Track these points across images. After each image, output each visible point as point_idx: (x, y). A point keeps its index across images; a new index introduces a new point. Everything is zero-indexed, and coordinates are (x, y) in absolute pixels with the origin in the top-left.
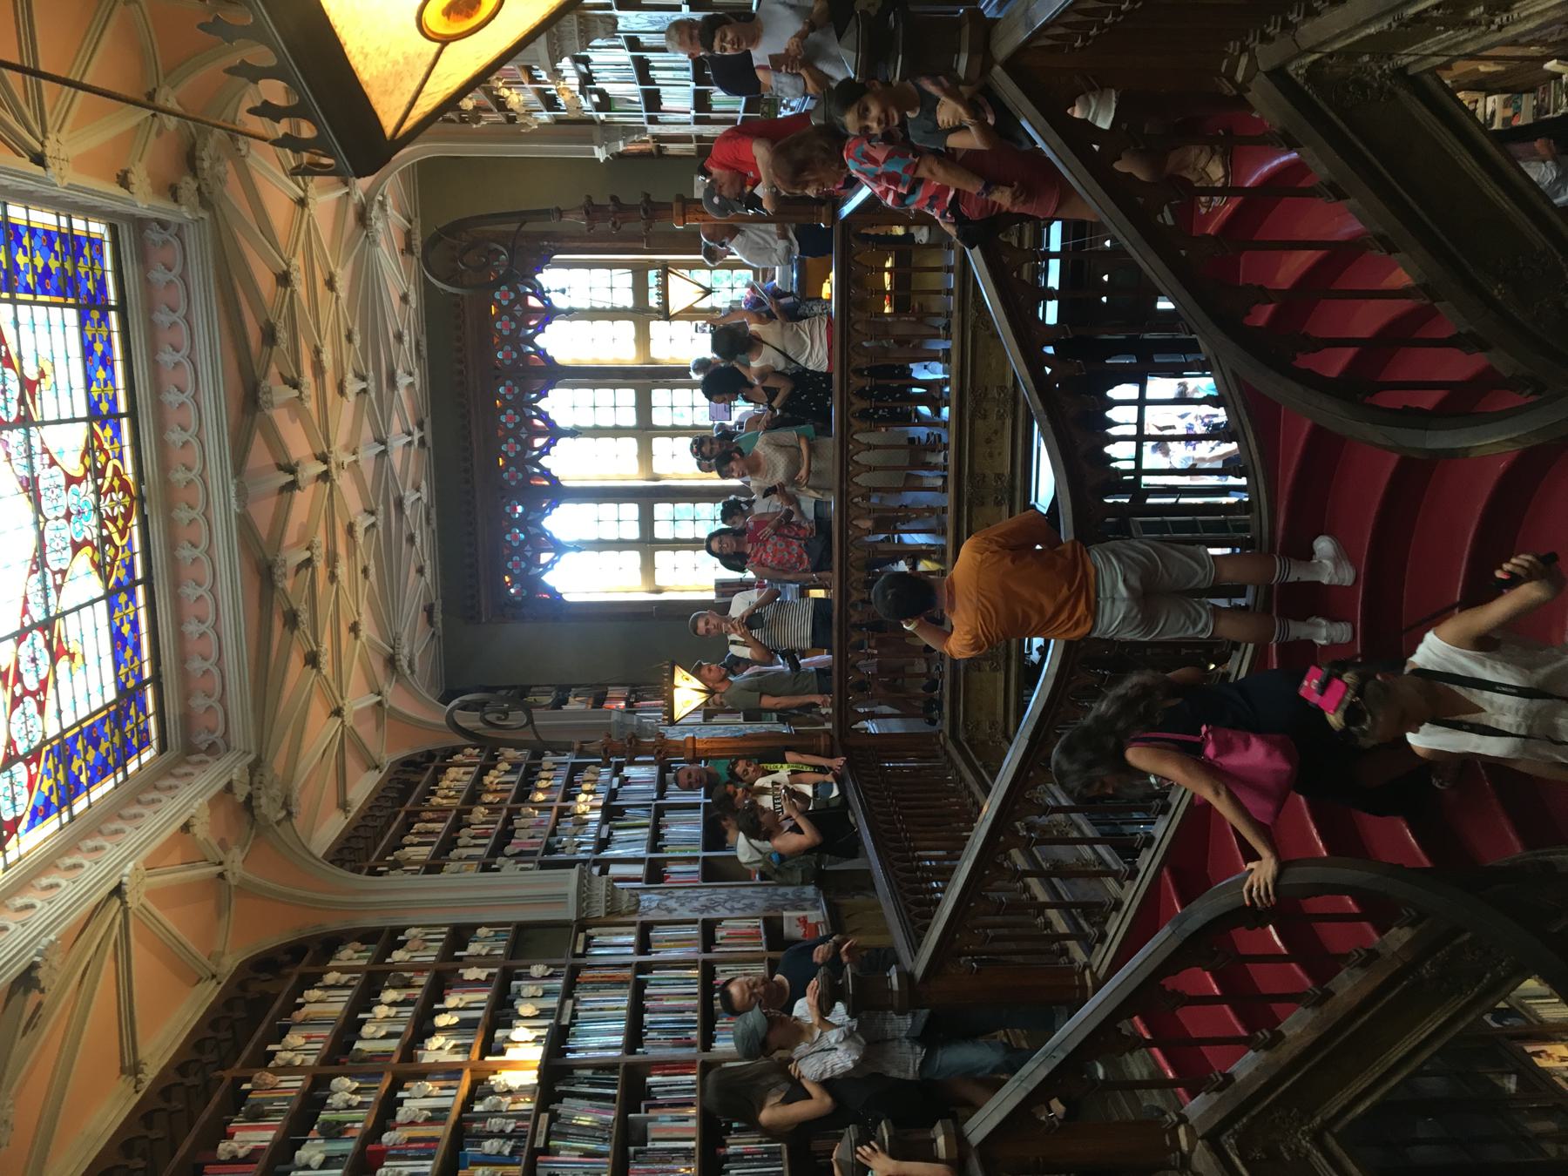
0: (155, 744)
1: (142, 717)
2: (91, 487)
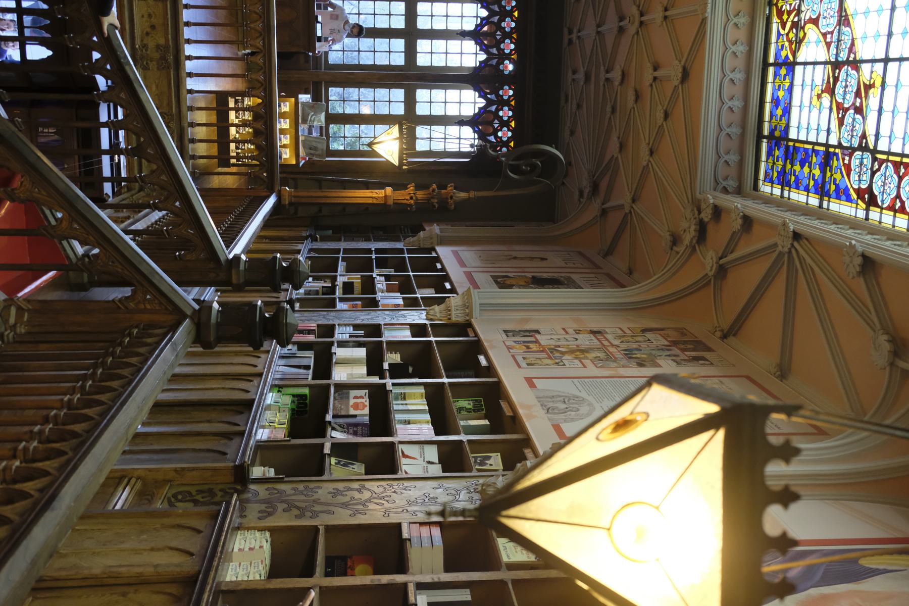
2: (802, 16)
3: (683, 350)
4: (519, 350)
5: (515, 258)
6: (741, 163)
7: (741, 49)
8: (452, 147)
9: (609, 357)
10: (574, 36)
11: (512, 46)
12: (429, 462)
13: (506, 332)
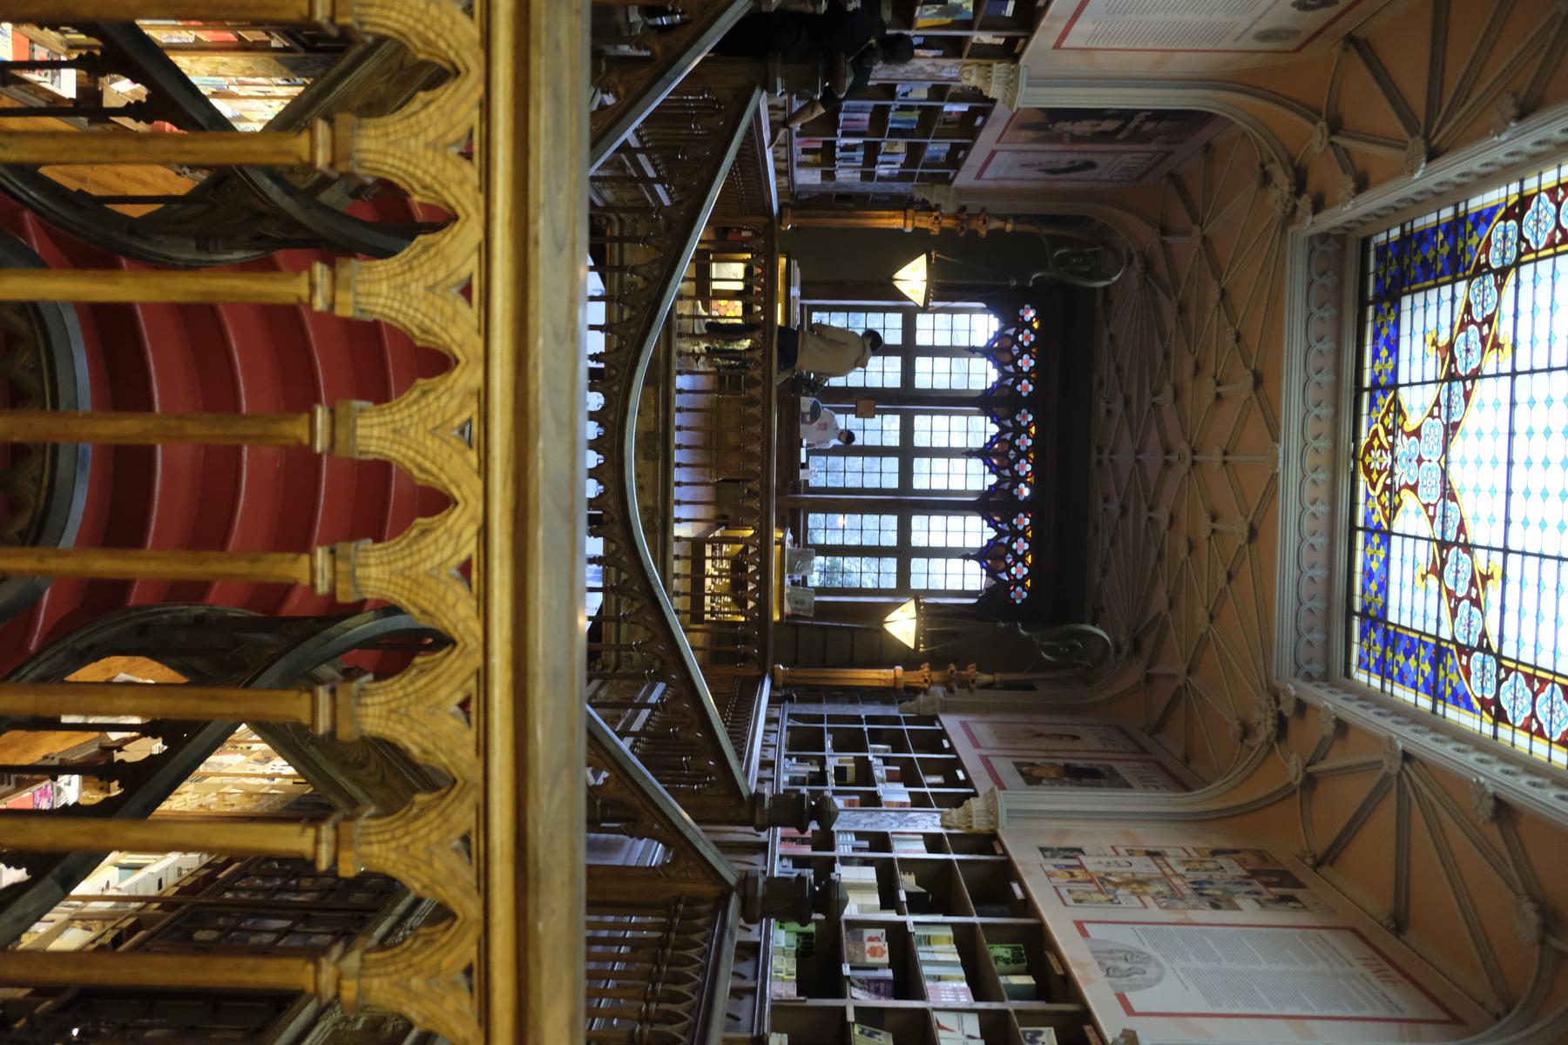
0: (1372, 247)
1: (1381, 273)
2: (1396, 479)
3: (1267, 885)
4: (1061, 878)
5: (1040, 735)
6: (1328, 643)
7: (1322, 509)
8: (954, 584)
9: (1175, 895)
10: (1106, 457)
11: (1029, 468)
12: (970, 1037)
13: (1042, 850)
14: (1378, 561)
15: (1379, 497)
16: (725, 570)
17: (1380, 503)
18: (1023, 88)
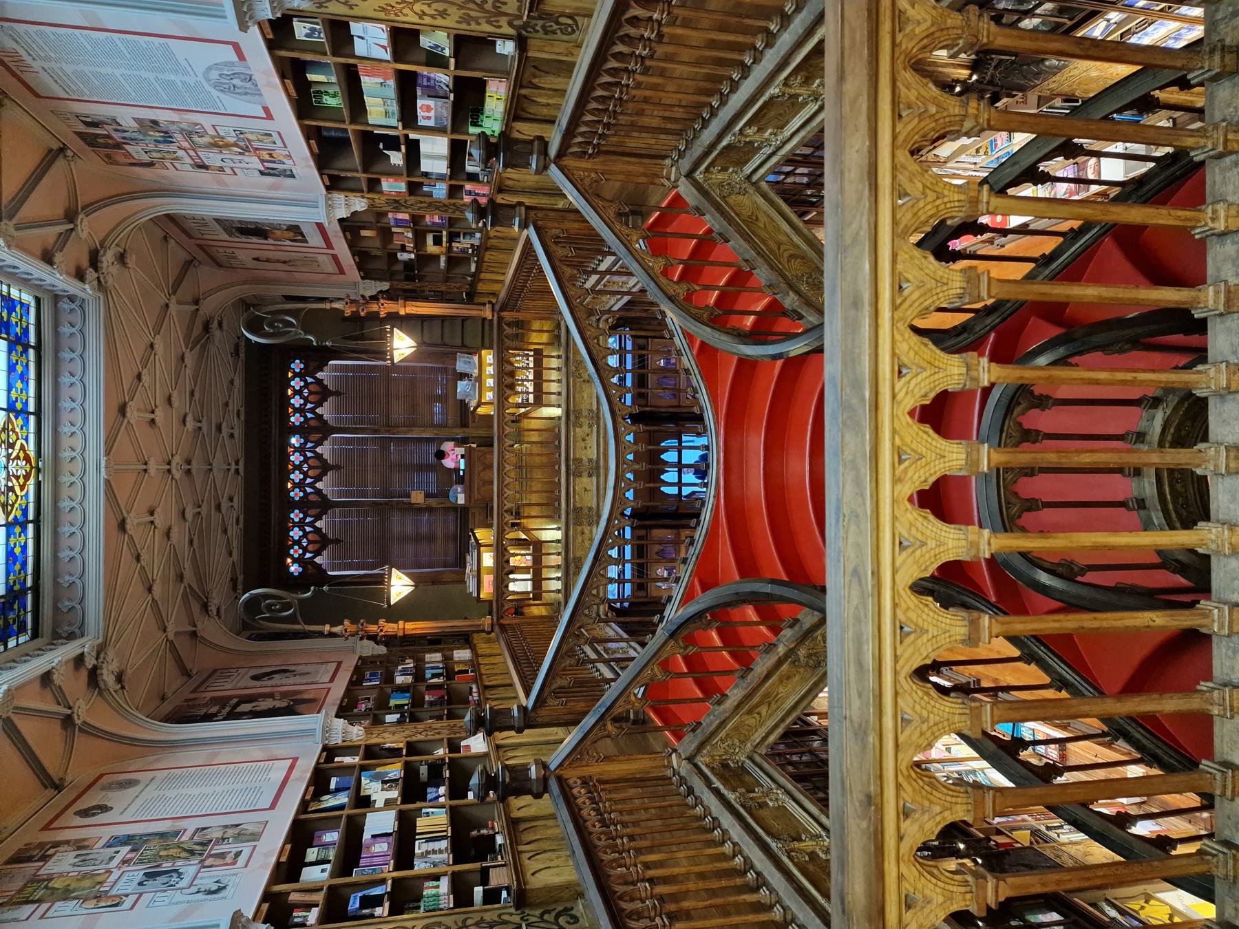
0: (29, 632)
1: (22, 612)
3: (109, 137)
4: (280, 153)
5: (285, 262)
6: (56, 324)
7: (66, 429)
9: (188, 135)
10: (233, 467)
11: (292, 458)
12: (362, 38)
13: (293, 176)
14: (16, 388)
15: (18, 439)
16: (519, 385)
17: (17, 435)
18: (319, 728)
